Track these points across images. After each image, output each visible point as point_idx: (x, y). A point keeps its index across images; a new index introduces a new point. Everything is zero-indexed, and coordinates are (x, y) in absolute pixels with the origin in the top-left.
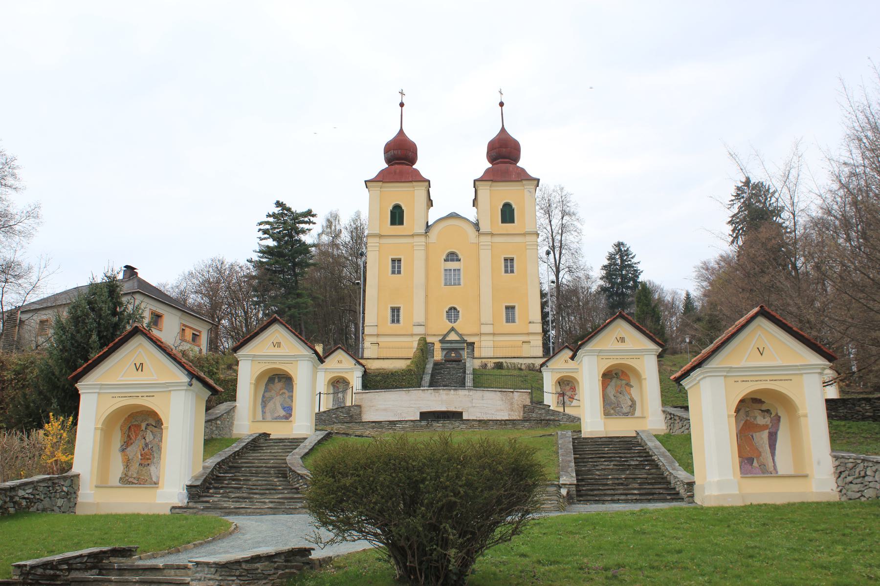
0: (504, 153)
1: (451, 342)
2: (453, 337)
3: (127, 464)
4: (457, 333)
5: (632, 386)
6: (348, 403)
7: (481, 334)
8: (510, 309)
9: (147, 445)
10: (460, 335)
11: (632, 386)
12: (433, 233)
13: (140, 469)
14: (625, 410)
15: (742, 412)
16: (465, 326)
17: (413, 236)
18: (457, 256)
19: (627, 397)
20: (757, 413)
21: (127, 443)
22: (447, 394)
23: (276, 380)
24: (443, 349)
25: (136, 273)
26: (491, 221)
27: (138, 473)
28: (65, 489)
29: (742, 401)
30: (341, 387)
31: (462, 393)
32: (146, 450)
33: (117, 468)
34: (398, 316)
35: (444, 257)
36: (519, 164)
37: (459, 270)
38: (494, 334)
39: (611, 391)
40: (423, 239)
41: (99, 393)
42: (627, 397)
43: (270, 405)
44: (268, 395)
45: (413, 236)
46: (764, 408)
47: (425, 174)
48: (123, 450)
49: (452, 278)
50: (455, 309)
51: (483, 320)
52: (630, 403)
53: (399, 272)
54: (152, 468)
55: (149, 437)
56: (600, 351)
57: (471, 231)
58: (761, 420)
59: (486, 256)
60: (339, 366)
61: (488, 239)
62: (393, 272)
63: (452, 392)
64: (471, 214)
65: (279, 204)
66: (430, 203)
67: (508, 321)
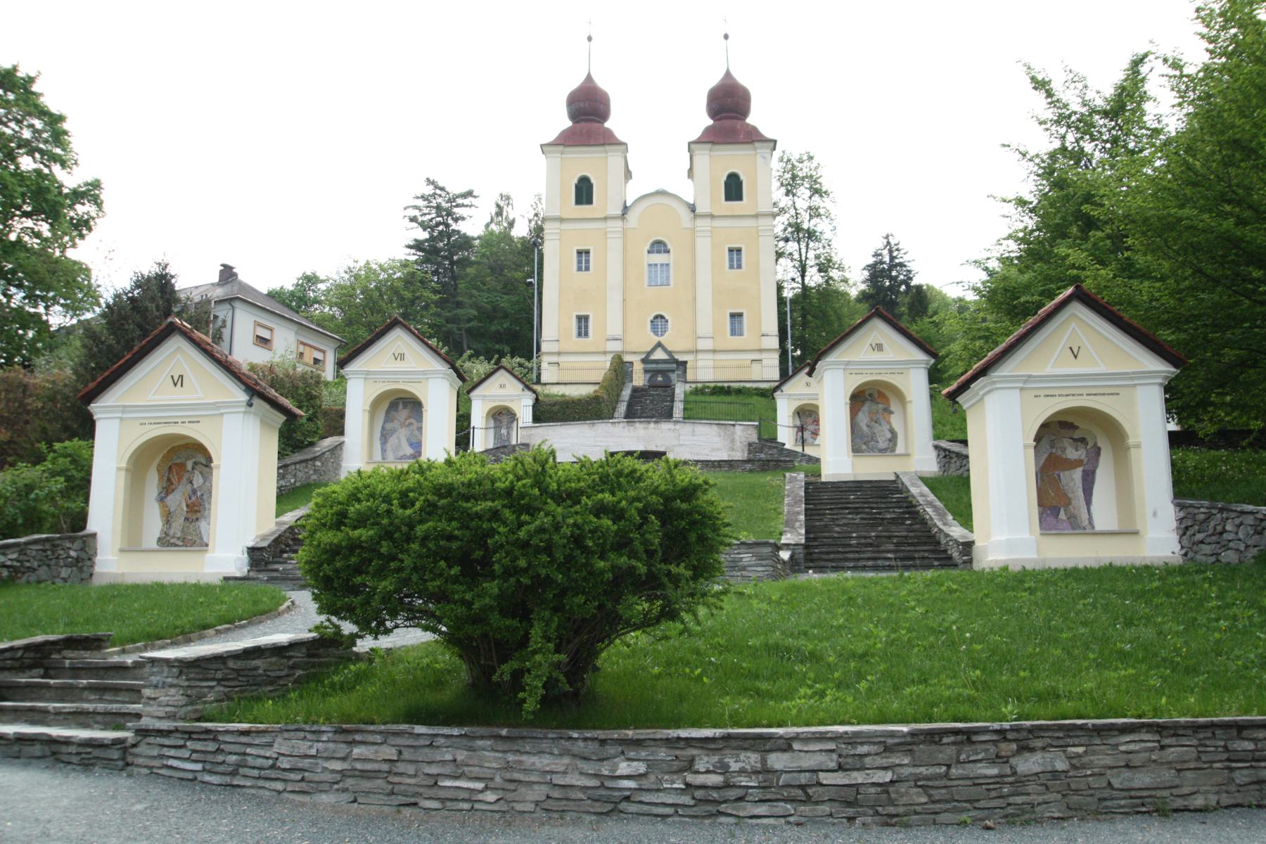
0: (728, 105)
1: (657, 362)
2: (659, 355)
3: (168, 517)
4: (665, 350)
5: (891, 413)
6: (514, 442)
7: (697, 351)
8: (736, 317)
9: (194, 492)
10: (669, 353)
11: (891, 413)
12: (632, 217)
13: (186, 528)
14: (882, 445)
15: (1045, 442)
16: (675, 340)
17: (605, 219)
18: (665, 245)
19: (886, 427)
20: (1066, 442)
21: (167, 489)
22: (645, 429)
23: (401, 406)
24: (646, 371)
25: (236, 275)
26: (711, 198)
27: (183, 531)
28: (72, 553)
29: (1045, 426)
30: (505, 419)
31: (665, 426)
32: (194, 498)
33: (153, 524)
34: (586, 327)
35: (648, 247)
36: (749, 120)
37: (668, 265)
38: (714, 351)
39: (863, 419)
40: (619, 223)
41: (121, 419)
42: (886, 427)
43: (392, 441)
44: (389, 426)
45: (605, 219)
46: (1077, 435)
47: (620, 135)
48: (161, 500)
49: (659, 276)
50: (662, 317)
51: (700, 333)
52: (889, 435)
53: (587, 269)
54: (203, 524)
55: (198, 480)
56: (848, 363)
57: (685, 214)
58: (1072, 454)
59: (704, 246)
60: (502, 392)
62: (580, 269)
63: (652, 425)
64: (687, 191)
65: (430, 182)
66: (628, 175)
67: (733, 333)
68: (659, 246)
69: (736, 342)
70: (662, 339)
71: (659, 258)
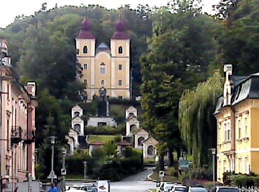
2: (103, 89)
8: (120, 81)
16: (106, 85)
17: (90, 57)
40: (94, 58)
45: (90, 57)
49: (103, 70)
61: (114, 59)
68: (103, 64)
69: (120, 87)
70: (103, 86)
71: (103, 66)
